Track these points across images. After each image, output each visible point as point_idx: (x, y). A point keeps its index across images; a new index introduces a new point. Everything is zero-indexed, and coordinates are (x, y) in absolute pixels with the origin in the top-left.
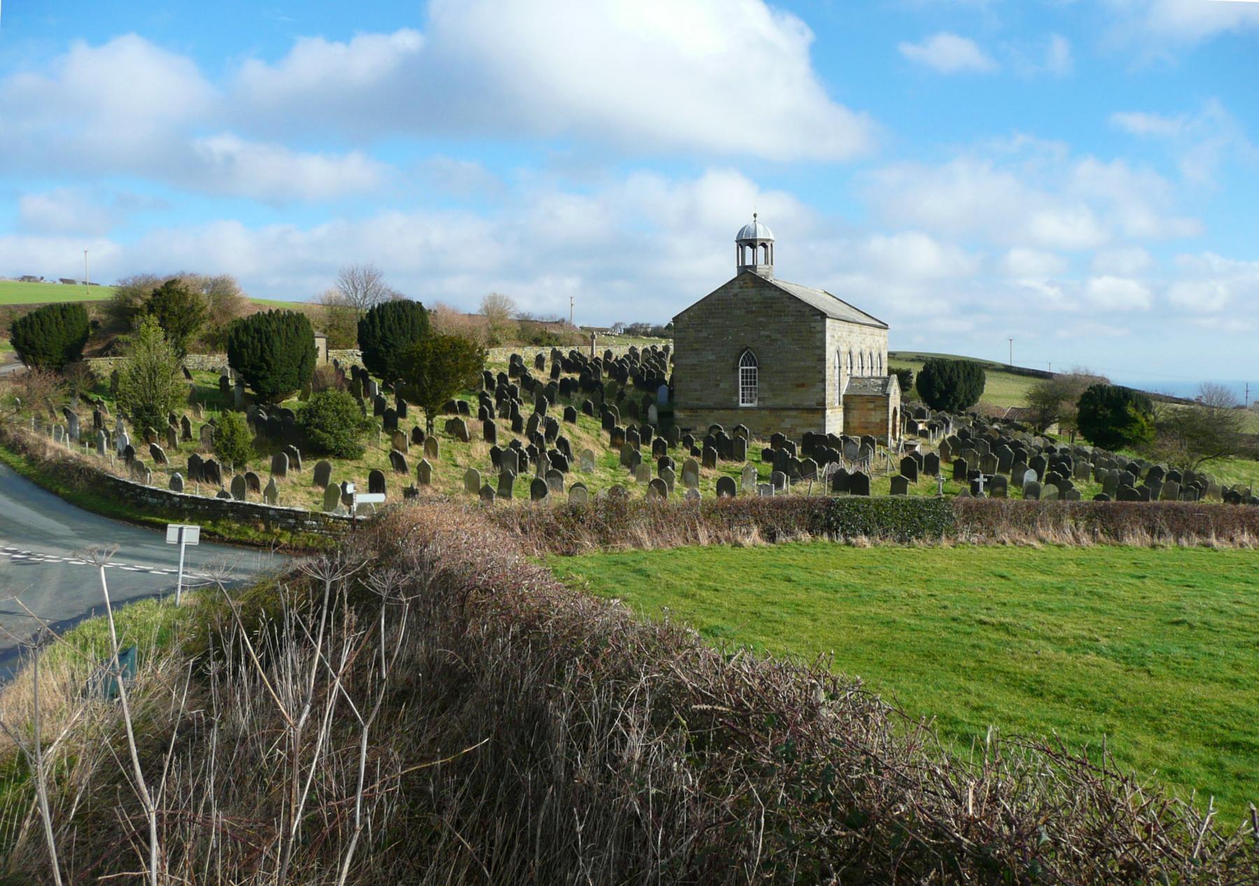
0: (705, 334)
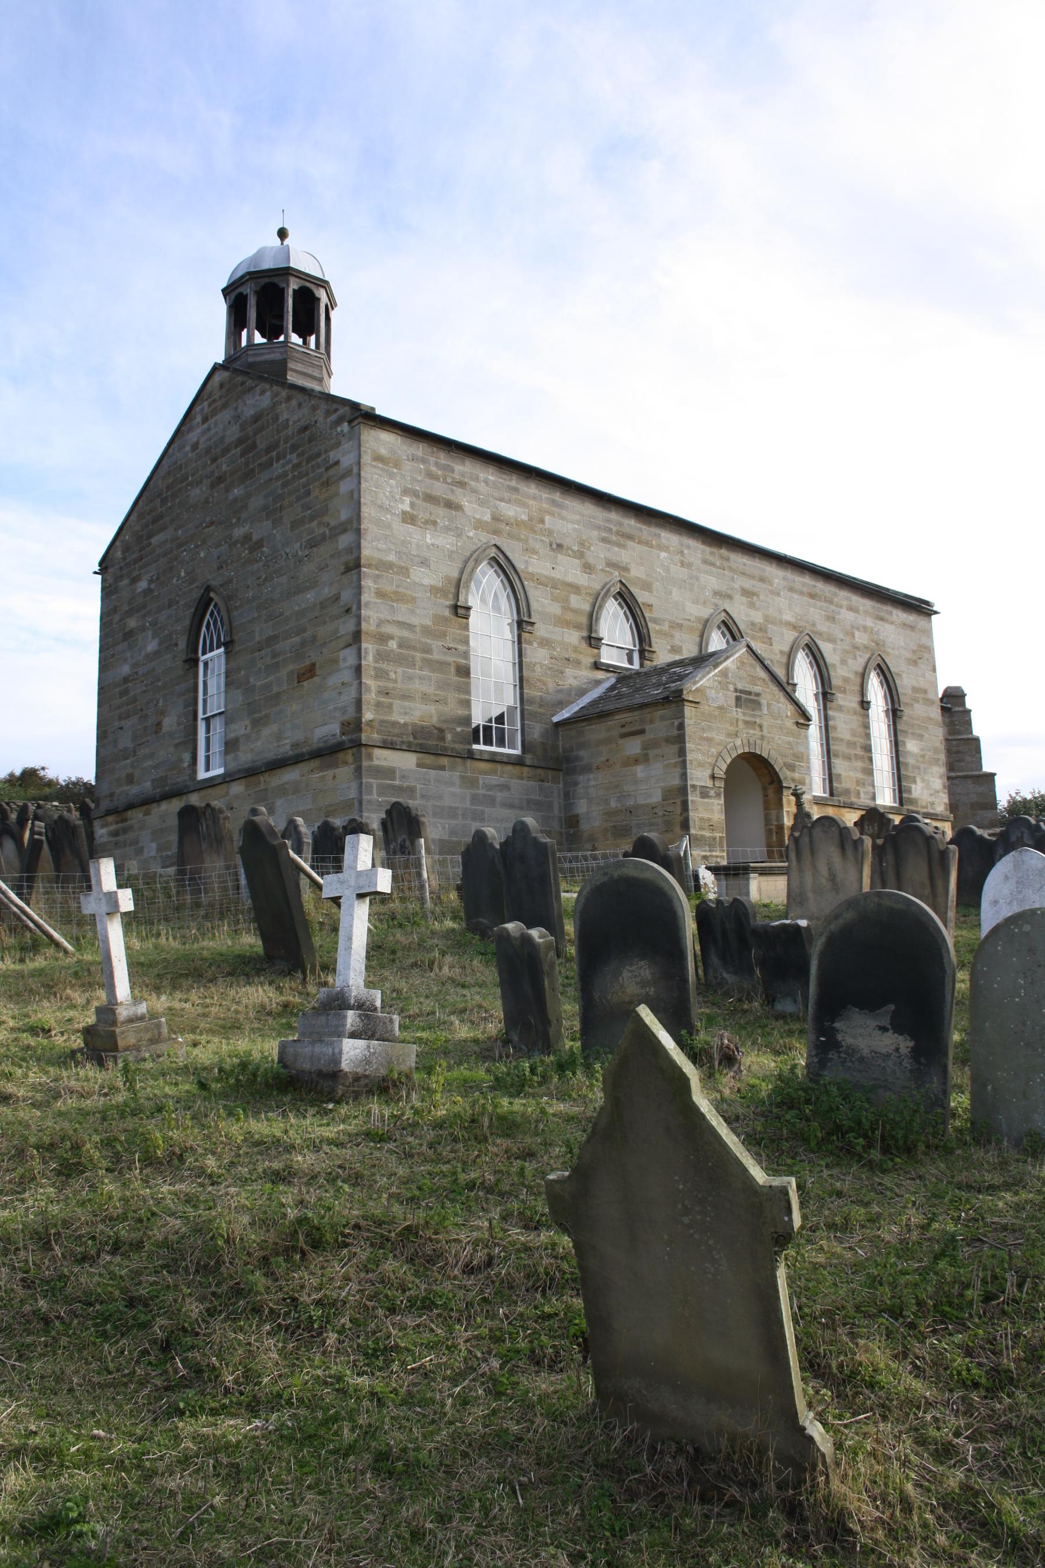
0: (143, 585)
